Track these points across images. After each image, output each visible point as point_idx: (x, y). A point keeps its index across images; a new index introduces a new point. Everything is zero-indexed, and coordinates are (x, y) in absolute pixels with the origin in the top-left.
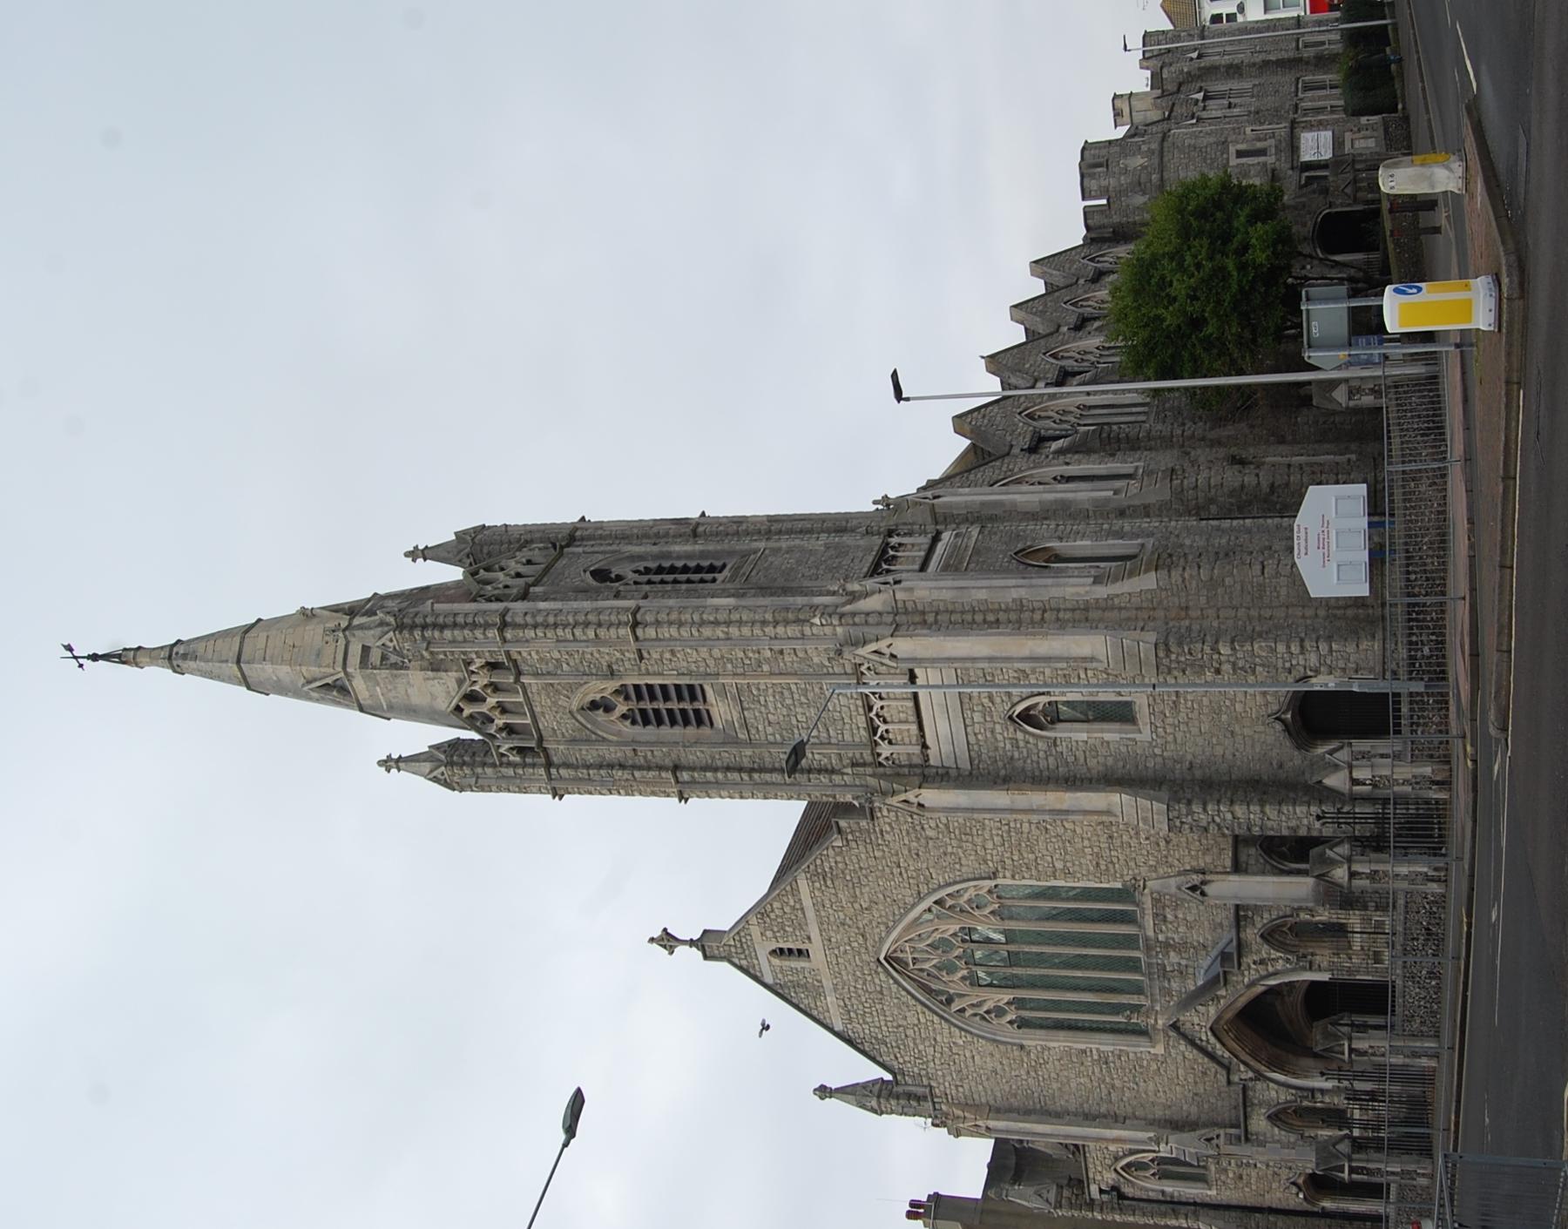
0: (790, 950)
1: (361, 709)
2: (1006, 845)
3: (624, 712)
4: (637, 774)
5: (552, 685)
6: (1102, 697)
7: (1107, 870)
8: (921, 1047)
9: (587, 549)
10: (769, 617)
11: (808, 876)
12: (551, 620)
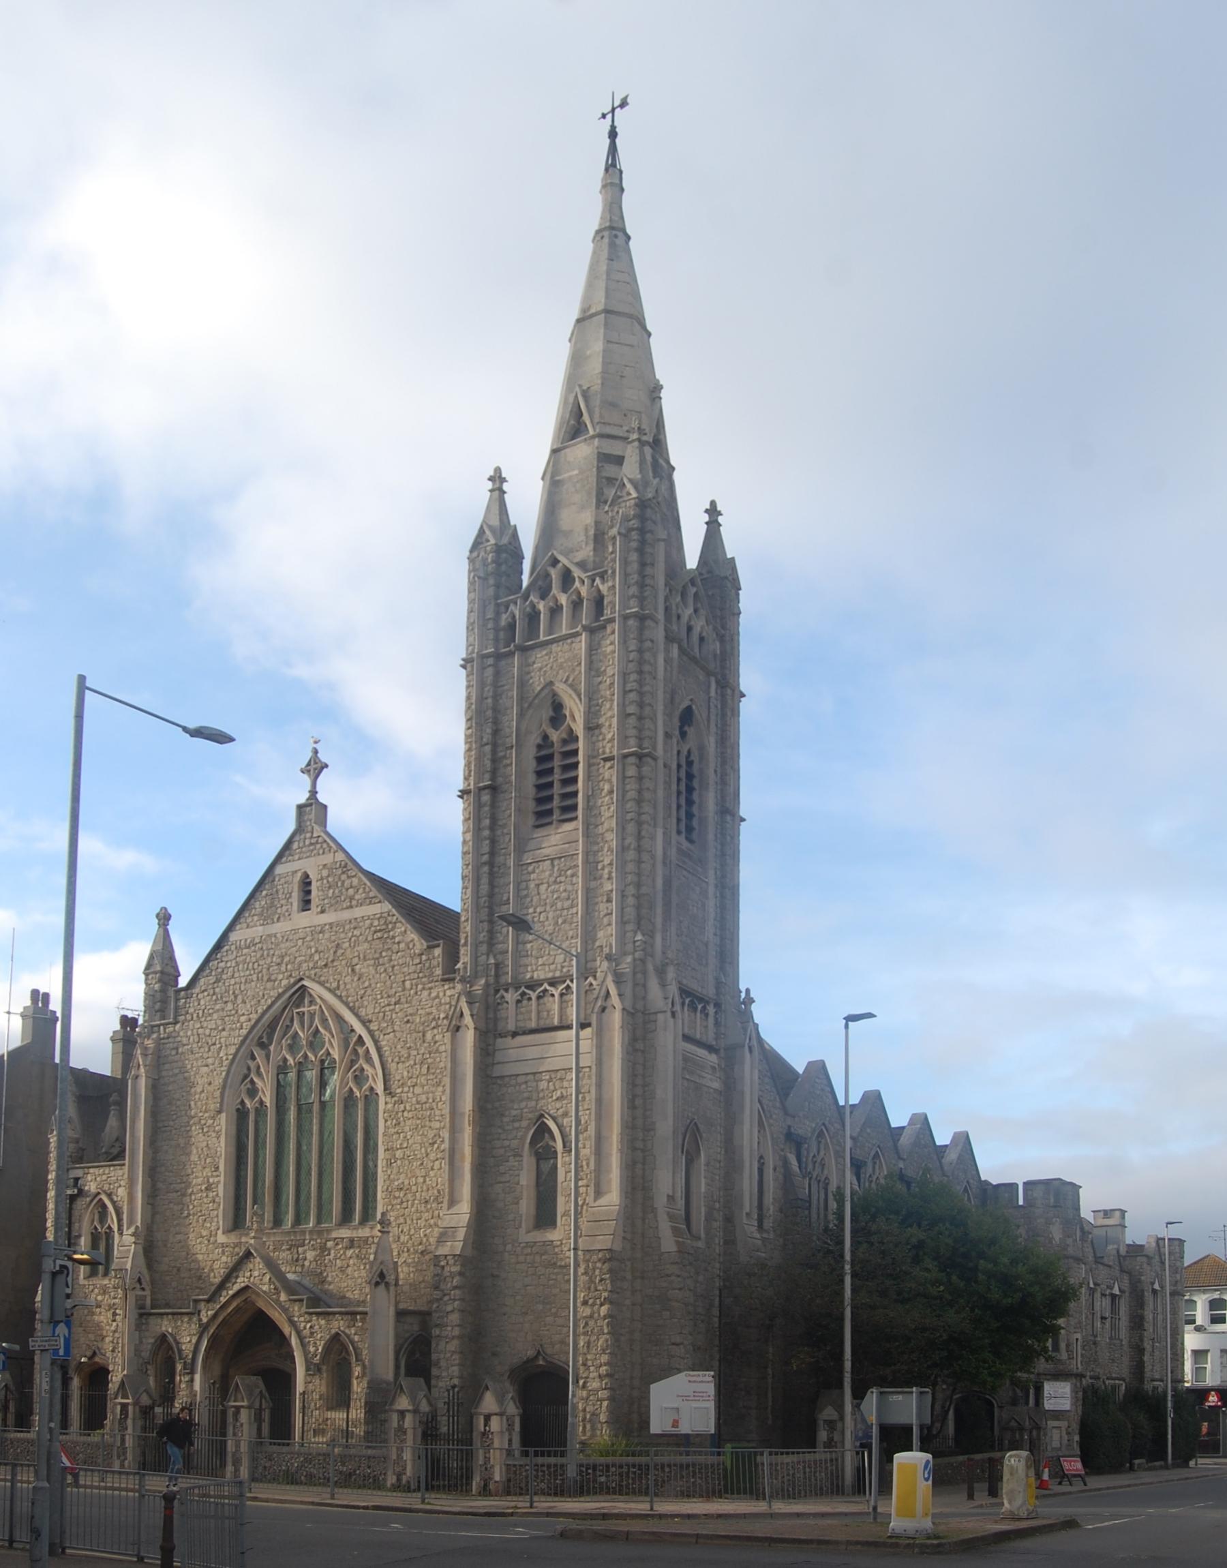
0: (309, 892)
1: (554, 452)
2: (417, 1106)
3: (551, 738)
4: (488, 748)
5: (580, 664)
6: (561, 1200)
7: (395, 1198)
8: (215, 1016)
9: (713, 700)
10: (644, 890)
11: (386, 915)
12: (646, 668)
